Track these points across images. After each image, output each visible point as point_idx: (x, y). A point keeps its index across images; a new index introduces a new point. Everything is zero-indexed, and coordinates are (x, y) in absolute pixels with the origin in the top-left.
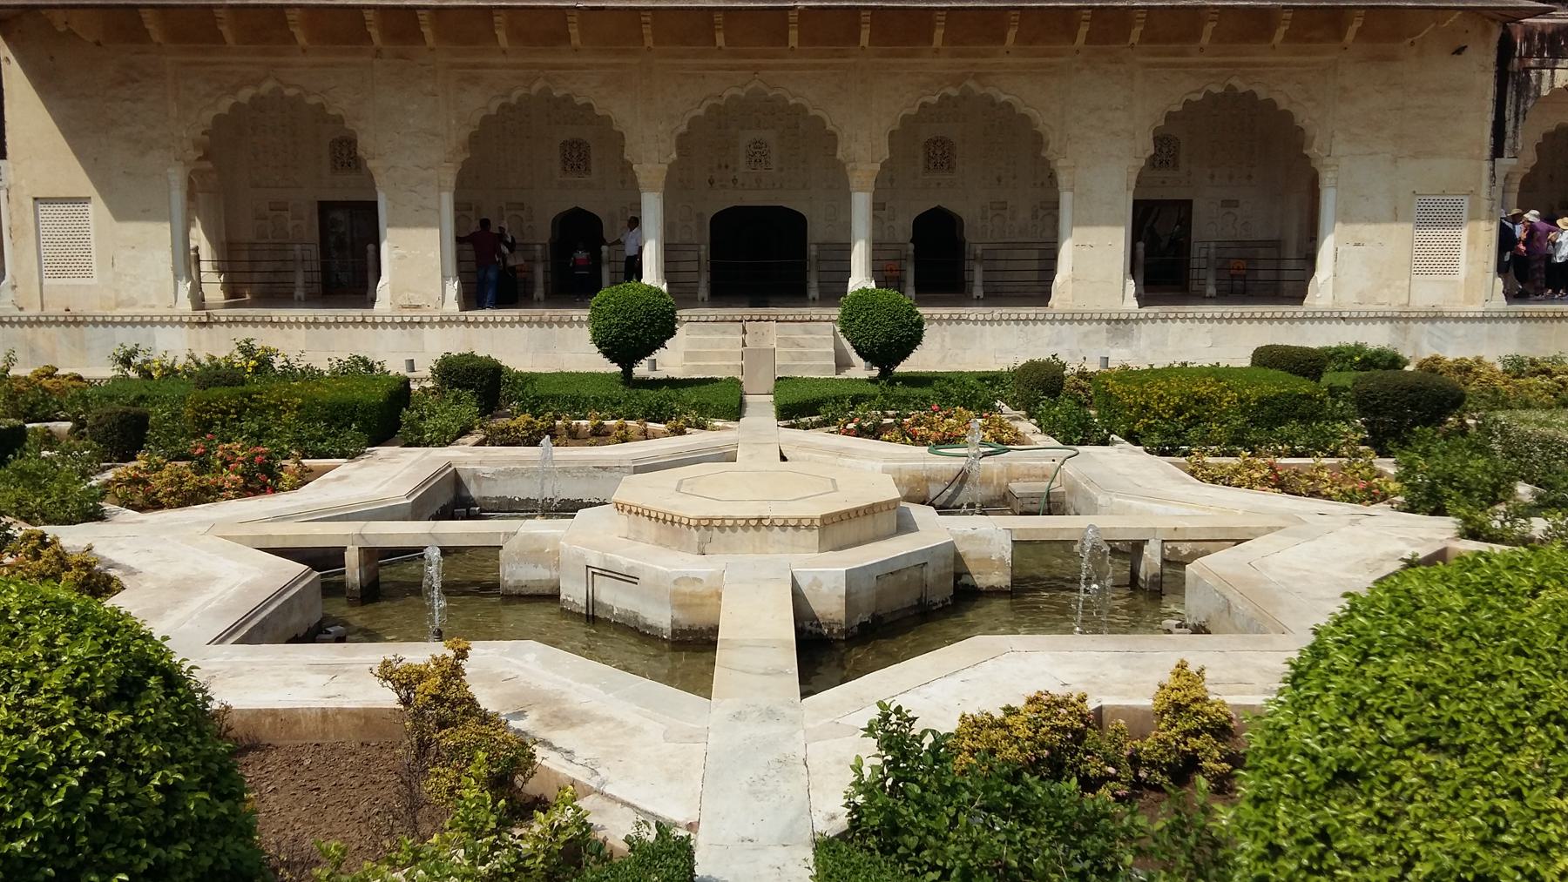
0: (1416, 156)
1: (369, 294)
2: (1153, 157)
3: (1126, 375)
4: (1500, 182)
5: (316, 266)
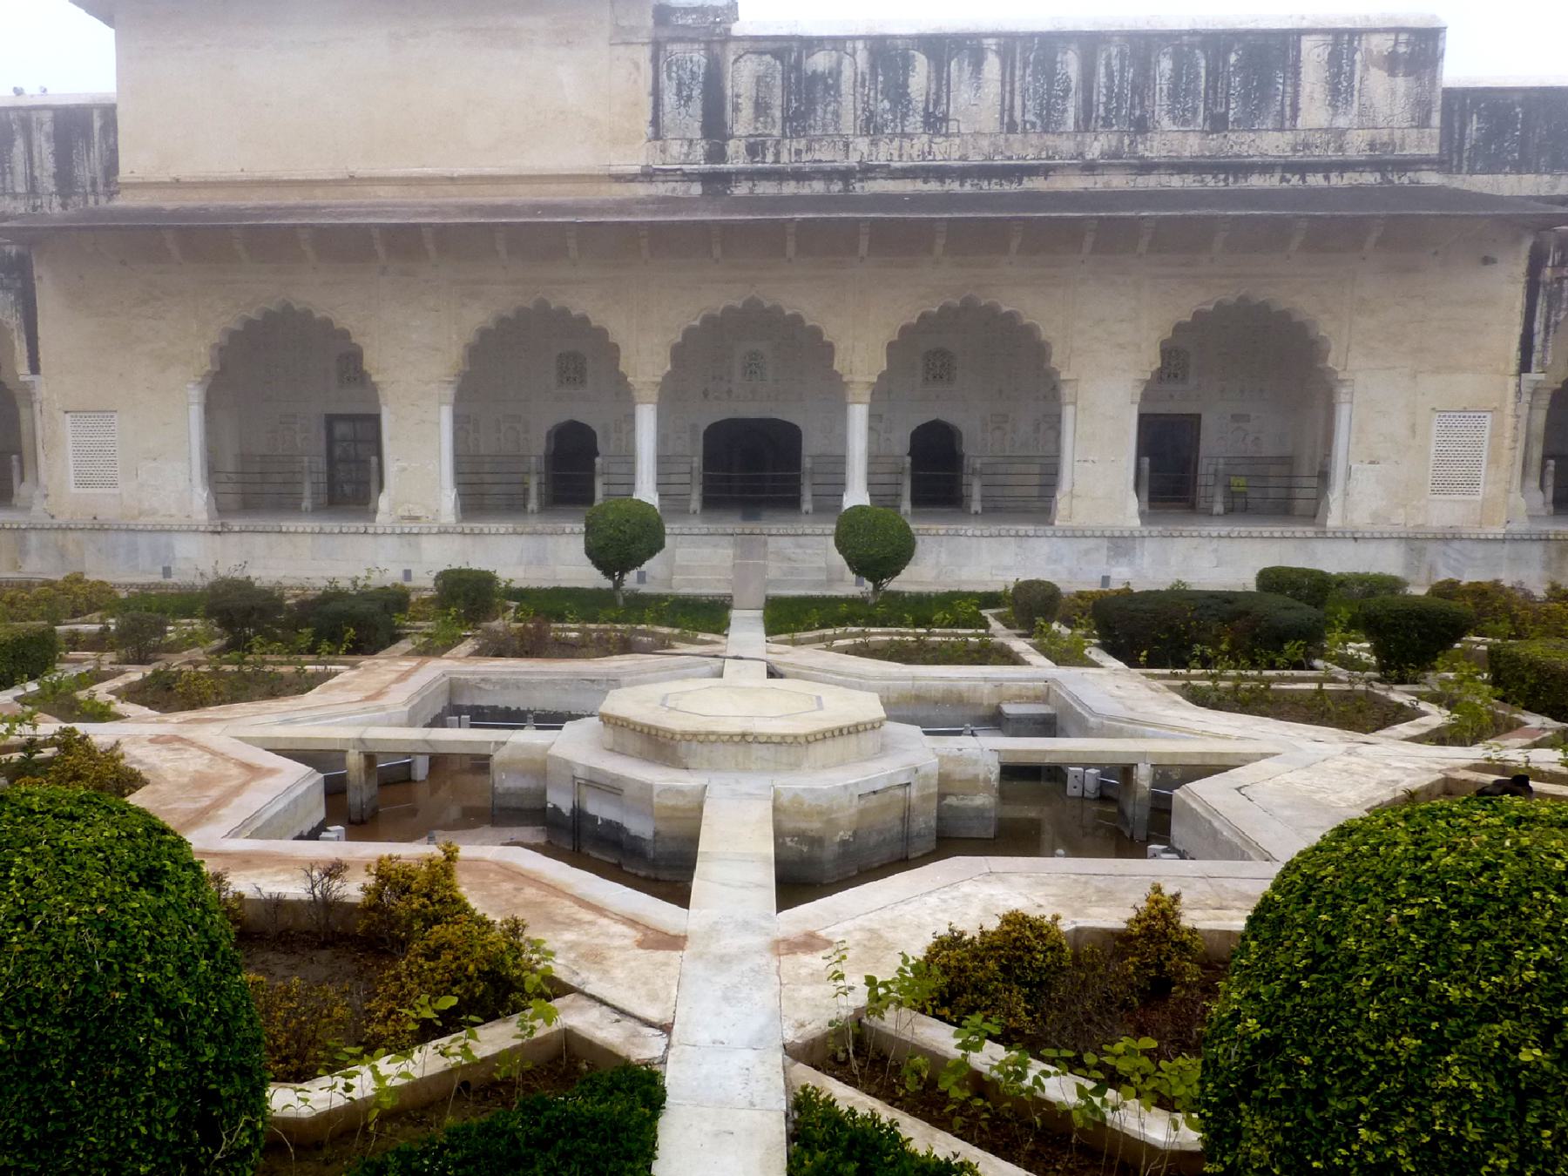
1: (371, 506)
2: (1160, 370)
3: (1127, 594)
4: (1526, 398)
5: (323, 478)
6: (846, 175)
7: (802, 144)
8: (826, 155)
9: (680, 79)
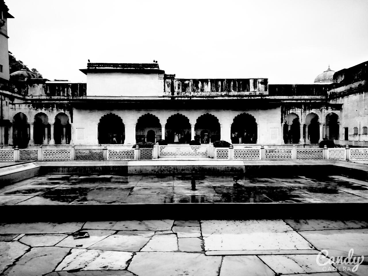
0: (270, 123)
6: (191, 97)
7: (184, 93)
8: (187, 94)
9: (168, 84)
